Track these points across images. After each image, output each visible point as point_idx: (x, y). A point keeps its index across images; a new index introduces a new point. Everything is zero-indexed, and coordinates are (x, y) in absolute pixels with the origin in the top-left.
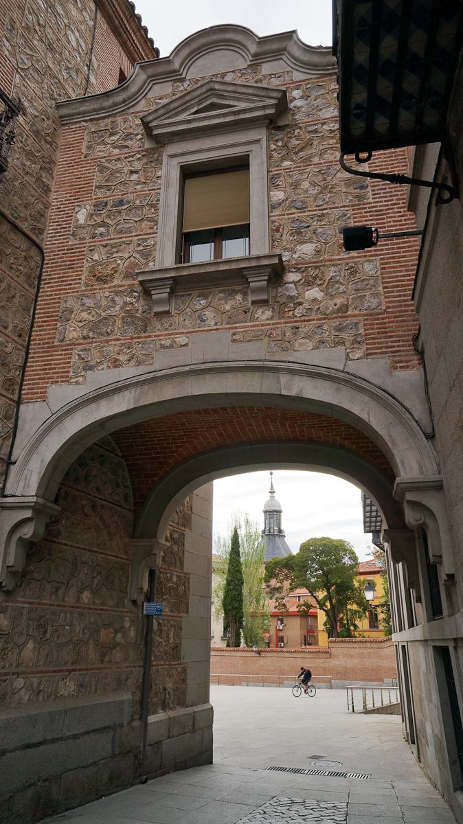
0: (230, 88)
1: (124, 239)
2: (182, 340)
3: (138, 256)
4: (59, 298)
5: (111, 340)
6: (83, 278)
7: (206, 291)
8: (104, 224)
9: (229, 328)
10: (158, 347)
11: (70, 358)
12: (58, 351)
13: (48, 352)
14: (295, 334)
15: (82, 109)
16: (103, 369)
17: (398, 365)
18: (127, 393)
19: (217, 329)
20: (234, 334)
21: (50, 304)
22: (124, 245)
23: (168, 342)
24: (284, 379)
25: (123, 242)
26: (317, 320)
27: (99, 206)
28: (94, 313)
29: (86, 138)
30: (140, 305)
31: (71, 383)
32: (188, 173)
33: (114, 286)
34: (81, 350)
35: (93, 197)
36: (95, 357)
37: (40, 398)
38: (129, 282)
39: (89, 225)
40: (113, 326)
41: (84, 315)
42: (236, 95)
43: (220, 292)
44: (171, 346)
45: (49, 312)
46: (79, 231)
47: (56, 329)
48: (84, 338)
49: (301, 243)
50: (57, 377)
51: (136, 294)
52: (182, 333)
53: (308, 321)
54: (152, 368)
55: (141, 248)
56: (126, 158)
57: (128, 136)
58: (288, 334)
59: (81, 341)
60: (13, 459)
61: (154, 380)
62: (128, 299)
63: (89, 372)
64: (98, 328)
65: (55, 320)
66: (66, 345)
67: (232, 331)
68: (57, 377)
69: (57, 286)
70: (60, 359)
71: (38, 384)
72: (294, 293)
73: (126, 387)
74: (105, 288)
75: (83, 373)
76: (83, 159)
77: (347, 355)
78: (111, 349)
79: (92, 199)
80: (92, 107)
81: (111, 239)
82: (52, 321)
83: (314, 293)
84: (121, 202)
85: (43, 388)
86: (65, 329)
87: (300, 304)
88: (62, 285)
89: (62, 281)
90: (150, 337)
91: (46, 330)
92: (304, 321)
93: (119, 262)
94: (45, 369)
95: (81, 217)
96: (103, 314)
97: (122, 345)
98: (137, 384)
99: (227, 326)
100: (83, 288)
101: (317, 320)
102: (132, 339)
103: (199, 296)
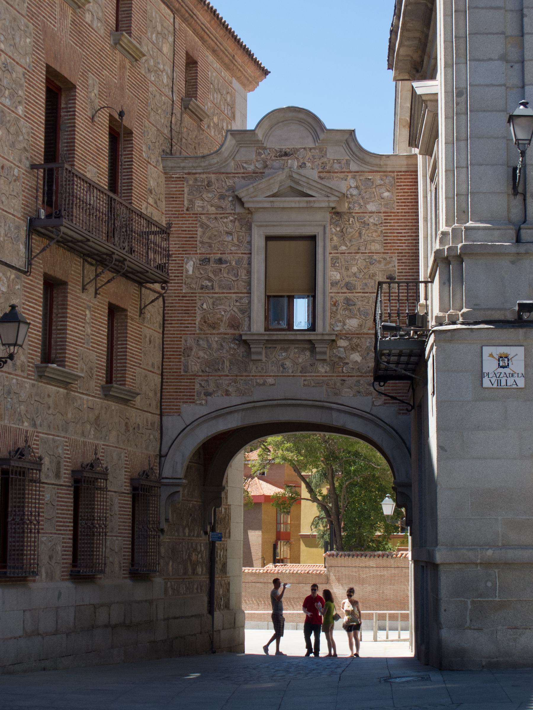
0: (304, 179)
1: (225, 295)
2: (270, 380)
3: (236, 310)
4: (181, 338)
5: (222, 375)
6: (197, 323)
7: (286, 346)
8: (210, 280)
9: (302, 376)
10: (255, 384)
11: (194, 386)
12: (184, 379)
13: (177, 379)
14: (342, 384)
15: (182, 165)
16: (218, 396)
17: (402, 412)
18: (236, 415)
19: (294, 376)
20: (305, 380)
21: (173, 341)
22: (226, 300)
23: (261, 382)
24: (335, 414)
25: (226, 297)
26: (357, 376)
27: (205, 261)
28: (208, 353)
29: (186, 190)
30: (242, 350)
31: (197, 404)
32: (268, 238)
33: (221, 334)
34: (202, 380)
35: (198, 251)
36: (211, 388)
37: (176, 412)
38: (232, 331)
39: (197, 278)
40: (222, 364)
41: (201, 354)
42: (308, 186)
43: (295, 348)
44: (264, 384)
45: (174, 348)
46: (189, 281)
47: (180, 362)
48: (202, 371)
49: (350, 318)
50: (187, 399)
51: (237, 342)
52: (271, 376)
53: (351, 376)
54: (250, 399)
55: (238, 304)
56: (221, 218)
57: (222, 197)
58: (338, 384)
59: (200, 374)
60: (163, 452)
61: (255, 406)
62: (232, 345)
63: (209, 397)
64: (212, 366)
65: (180, 355)
66: (190, 375)
67: (303, 378)
68: (187, 399)
69: (177, 327)
70: (187, 386)
71: (173, 402)
72: (343, 356)
73: (235, 411)
74: (214, 334)
75: (205, 398)
76: (185, 212)
77: (373, 402)
78: (225, 381)
79: (197, 254)
80: (191, 165)
81: (215, 293)
82: (177, 355)
83: (356, 357)
84: (220, 261)
85: (177, 405)
86: (188, 362)
87: (347, 363)
88: (181, 327)
89: (181, 324)
90: (249, 376)
91: (173, 362)
92: (349, 376)
93: (223, 313)
94: (177, 392)
95: (190, 267)
96: (215, 354)
97: (231, 379)
98: (243, 410)
99: (300, 374)
100: (198, 332)
101: (357, 376)
102: (237, 376)
103: (281, 349)
